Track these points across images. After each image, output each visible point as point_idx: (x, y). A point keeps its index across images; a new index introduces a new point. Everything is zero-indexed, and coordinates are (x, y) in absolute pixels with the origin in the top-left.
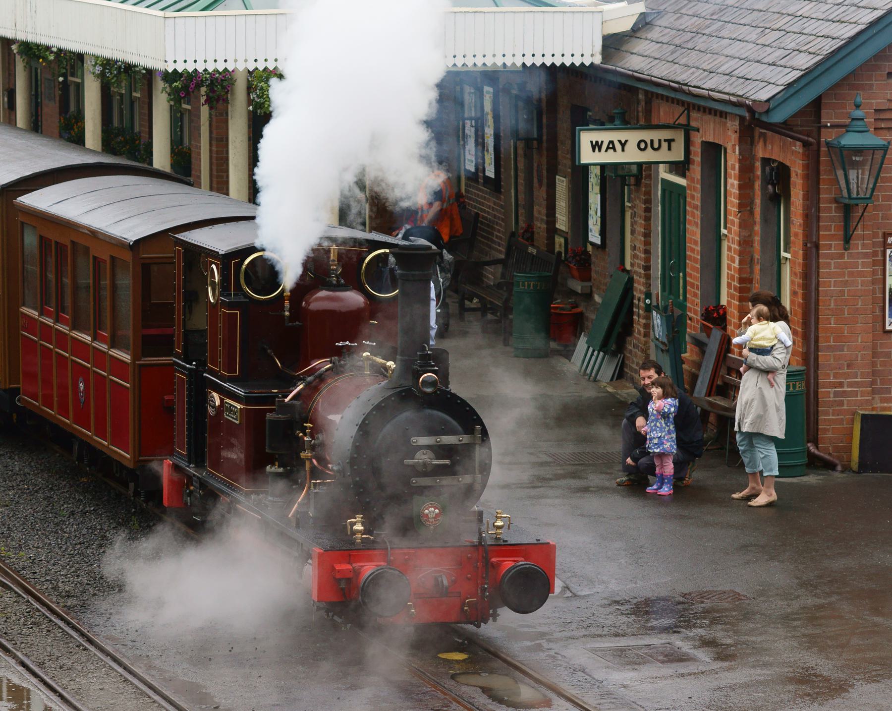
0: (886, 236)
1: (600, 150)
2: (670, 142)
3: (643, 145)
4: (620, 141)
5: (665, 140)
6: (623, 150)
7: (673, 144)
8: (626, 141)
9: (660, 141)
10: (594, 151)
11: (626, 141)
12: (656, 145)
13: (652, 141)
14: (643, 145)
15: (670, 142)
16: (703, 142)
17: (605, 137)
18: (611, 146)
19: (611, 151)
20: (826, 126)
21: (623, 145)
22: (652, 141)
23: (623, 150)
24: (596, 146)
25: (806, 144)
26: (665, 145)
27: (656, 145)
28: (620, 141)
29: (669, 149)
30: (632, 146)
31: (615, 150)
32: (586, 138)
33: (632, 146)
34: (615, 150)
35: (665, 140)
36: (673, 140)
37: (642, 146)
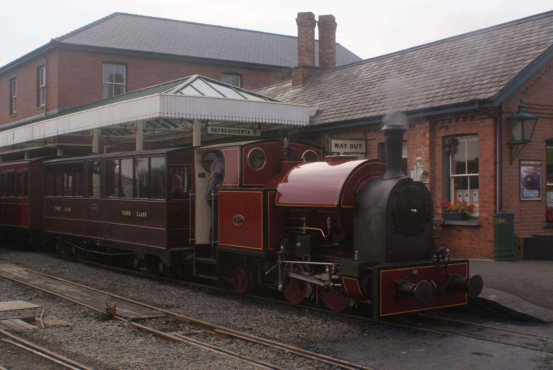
0: (520, 160)
1: (338, 147)
2: (360, 145)
3: (352, 146)
4: (344, 144)
5: (359, 145)
6: (345, 148)
7: (361, 146)
8: (346, 144)
9: (357, 145)
10: (336, 147)
11: (346, 144)
12: (356, 146)
13: (355, 145)
14: (352, 146)
15: (360, 145)
16: (379, 144)
17: (339, 142)
18: (341, 146)
19: (341, 148)
20: (504, 112)
21: (345, 145)
22: (355, 145)
23: (345, 148)
24: (337, 146)
25: (495, 120)
26: (359, 146)
27: (356, 146)
28: (344, 144)
29: (360, 148)
30: (348, 146)
31: (343, 148)
32: (334, 142)
33: (348, 146)
34: (343, 148)
35: (359, 145)
36: (361, 145)
37: (352, 146)
